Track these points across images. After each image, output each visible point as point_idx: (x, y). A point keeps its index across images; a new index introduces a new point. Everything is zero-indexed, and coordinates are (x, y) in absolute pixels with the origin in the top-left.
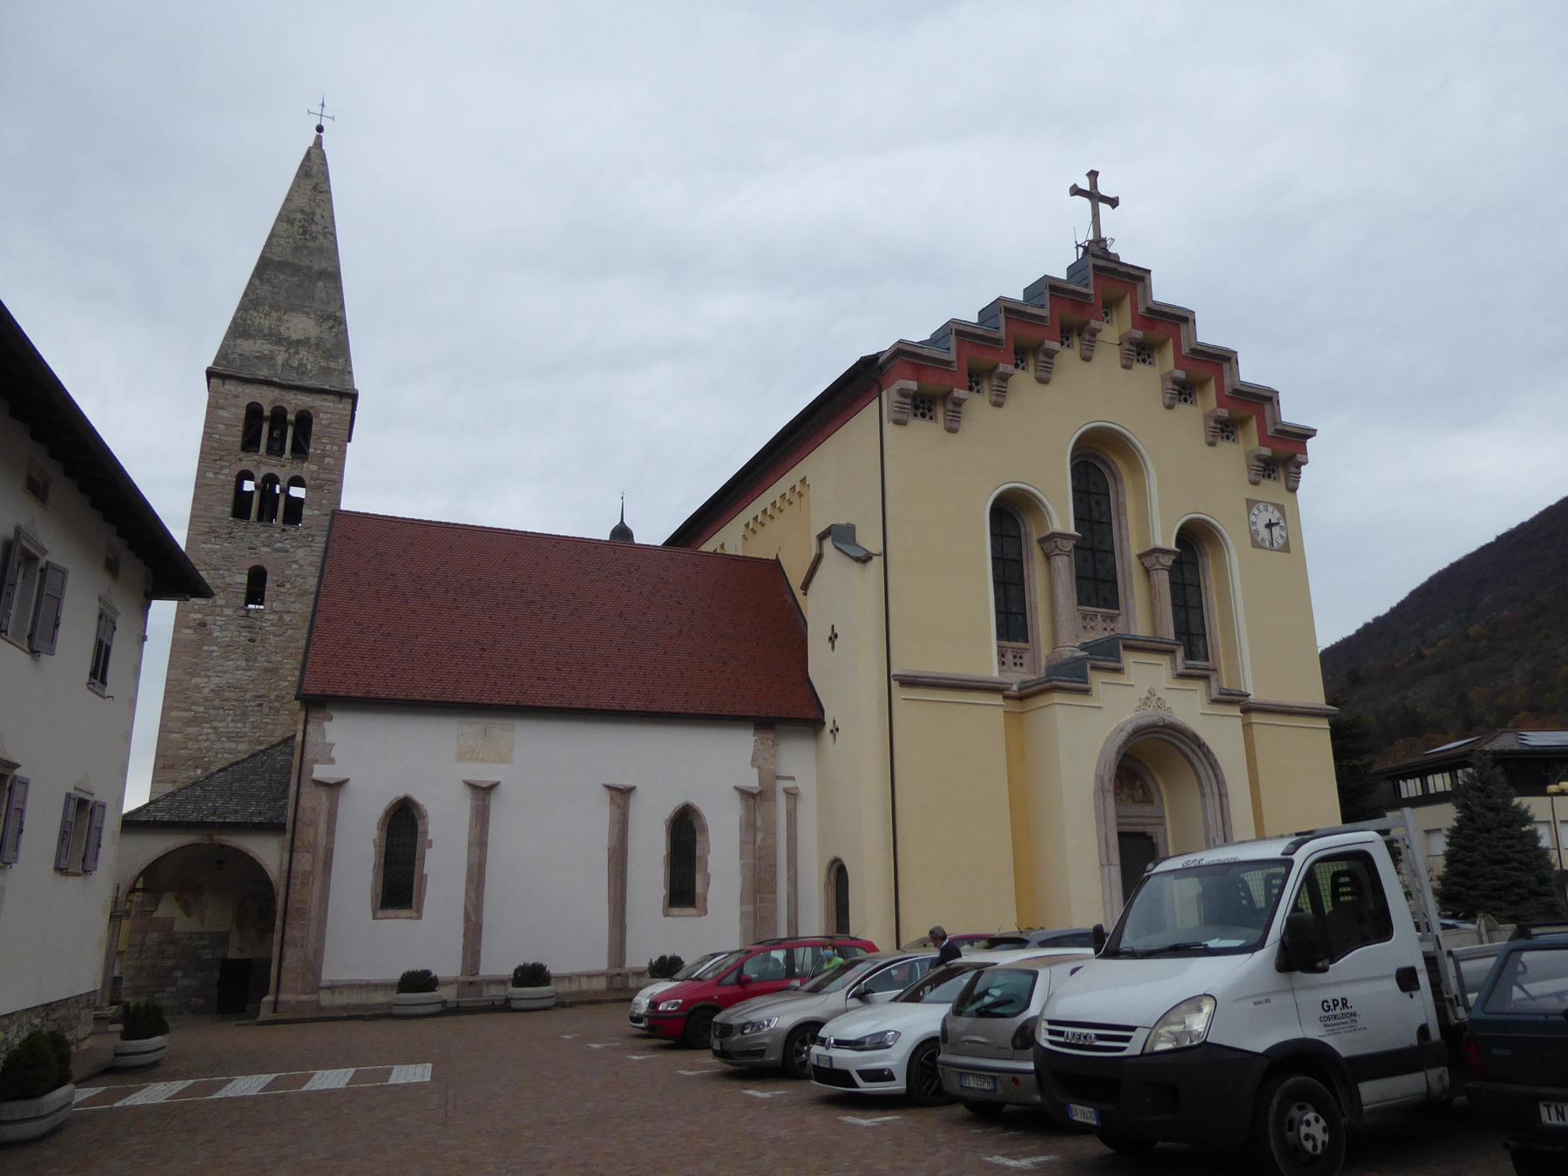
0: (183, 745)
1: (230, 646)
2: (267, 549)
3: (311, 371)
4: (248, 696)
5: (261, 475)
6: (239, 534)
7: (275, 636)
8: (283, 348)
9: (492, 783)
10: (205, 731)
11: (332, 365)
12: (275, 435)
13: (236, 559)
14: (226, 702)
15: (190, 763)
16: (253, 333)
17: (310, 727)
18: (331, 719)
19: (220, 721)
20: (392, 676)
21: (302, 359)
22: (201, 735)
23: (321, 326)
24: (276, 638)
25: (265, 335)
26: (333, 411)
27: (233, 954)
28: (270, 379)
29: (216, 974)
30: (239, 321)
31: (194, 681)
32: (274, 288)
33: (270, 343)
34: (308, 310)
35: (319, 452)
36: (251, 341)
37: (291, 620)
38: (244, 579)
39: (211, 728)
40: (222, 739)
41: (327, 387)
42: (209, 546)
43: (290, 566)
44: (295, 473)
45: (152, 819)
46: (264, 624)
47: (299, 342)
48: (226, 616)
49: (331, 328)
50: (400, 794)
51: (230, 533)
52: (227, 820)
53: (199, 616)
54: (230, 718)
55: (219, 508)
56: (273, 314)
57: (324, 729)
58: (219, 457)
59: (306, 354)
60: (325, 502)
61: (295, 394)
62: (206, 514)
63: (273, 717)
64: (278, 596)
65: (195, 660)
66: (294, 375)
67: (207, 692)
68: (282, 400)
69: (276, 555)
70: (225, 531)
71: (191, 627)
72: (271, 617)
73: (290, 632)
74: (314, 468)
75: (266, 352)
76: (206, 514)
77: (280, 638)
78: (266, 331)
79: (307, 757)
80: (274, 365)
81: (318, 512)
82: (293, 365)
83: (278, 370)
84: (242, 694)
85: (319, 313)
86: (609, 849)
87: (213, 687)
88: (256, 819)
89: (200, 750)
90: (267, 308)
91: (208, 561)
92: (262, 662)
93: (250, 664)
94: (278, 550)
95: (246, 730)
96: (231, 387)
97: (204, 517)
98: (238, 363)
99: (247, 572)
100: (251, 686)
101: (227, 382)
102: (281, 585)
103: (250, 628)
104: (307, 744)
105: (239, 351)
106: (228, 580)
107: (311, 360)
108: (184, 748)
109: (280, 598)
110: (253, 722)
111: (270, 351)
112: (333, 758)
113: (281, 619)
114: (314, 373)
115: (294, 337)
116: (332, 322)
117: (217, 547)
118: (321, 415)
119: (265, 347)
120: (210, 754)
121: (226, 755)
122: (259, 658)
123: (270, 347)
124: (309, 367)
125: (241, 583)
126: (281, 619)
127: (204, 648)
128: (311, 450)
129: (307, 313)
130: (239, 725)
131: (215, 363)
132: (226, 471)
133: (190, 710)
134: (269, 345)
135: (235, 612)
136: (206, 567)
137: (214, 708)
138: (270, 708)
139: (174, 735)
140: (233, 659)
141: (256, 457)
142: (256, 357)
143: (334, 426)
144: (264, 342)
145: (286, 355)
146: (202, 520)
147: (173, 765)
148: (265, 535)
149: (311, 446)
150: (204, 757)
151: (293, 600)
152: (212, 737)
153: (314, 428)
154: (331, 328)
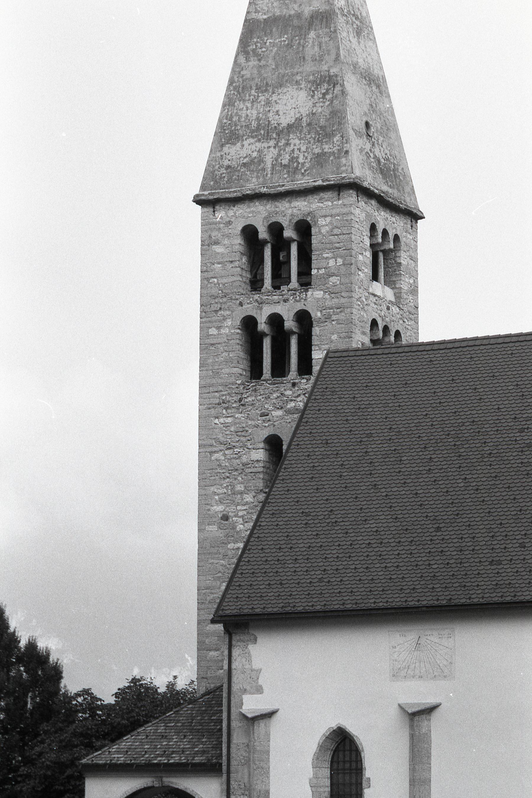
2: (280, 413)
3: (303, 164)
6: (250, 399)
8: (272, 143)
9: (427, 706)
11: (327, 148)
12: (281, 258)
16: (241, 132)
17: (236, 652)
18: (255, 641)
20: (320, 580)
21: (293, 150)
23: (313, 96)
25: (253, 131)
26: (334, 212)
28: (257, 191)
30: (225, 121)
32: (259, 60)
33: (259, 140)
34: (298, 78)
35: (322, 271)
36: (239, 144)
41: (320, 183)
42: (222, 420)
44: (299, 306)
45: (108, 762)
47: (290, 127)
48: (247, 503)
49: (324, 95)
50: (334, 725)
51: (240, 400)
52: (170, 762)
56: (262, 98)
57: (249, 653)
59: (297, 142)
66: (286, 176)
70: (235, 398)
74: (319, 294)
75: (255, 154)
76: (214, 381)
78: (254, 124)
79: (235, 687)
80: (264, 169)
82: (284, 162)
83: (267, 174)
85: (311, 78)
88: (198, 759)
90: (253, 92)
91: (222, 439)
96: (221, 214)
97: (212, 385)
98: (226, 179)
99: (262, 445)
101: (217, 207)
104: (234, 672)
105: (226, 163)
106: (244, 459)
107: (303, 149)
111: (259, 151)
112: (261, 687)
114: (307, 165)
115: (285, 121)
116: (326, 86)
117: (230, 420)
118: (321, 222)
119: (253, 147)
123: (259, 145)
124: (301, 160)
125: (258, 461)
127: (229, 546)
128: (314, 272)
129: (297, 83)
131: (203, 187)
132: (229, 322)
134: (257, 144)
135: (254, 497)
136: (222, 447)
141: (256, 297)
142: (244, 165)
143: (336, 231)
144: (252, 140)
145: (276, 152)
149: (313, 266)
153: (315, 241)
154: (324, 95)
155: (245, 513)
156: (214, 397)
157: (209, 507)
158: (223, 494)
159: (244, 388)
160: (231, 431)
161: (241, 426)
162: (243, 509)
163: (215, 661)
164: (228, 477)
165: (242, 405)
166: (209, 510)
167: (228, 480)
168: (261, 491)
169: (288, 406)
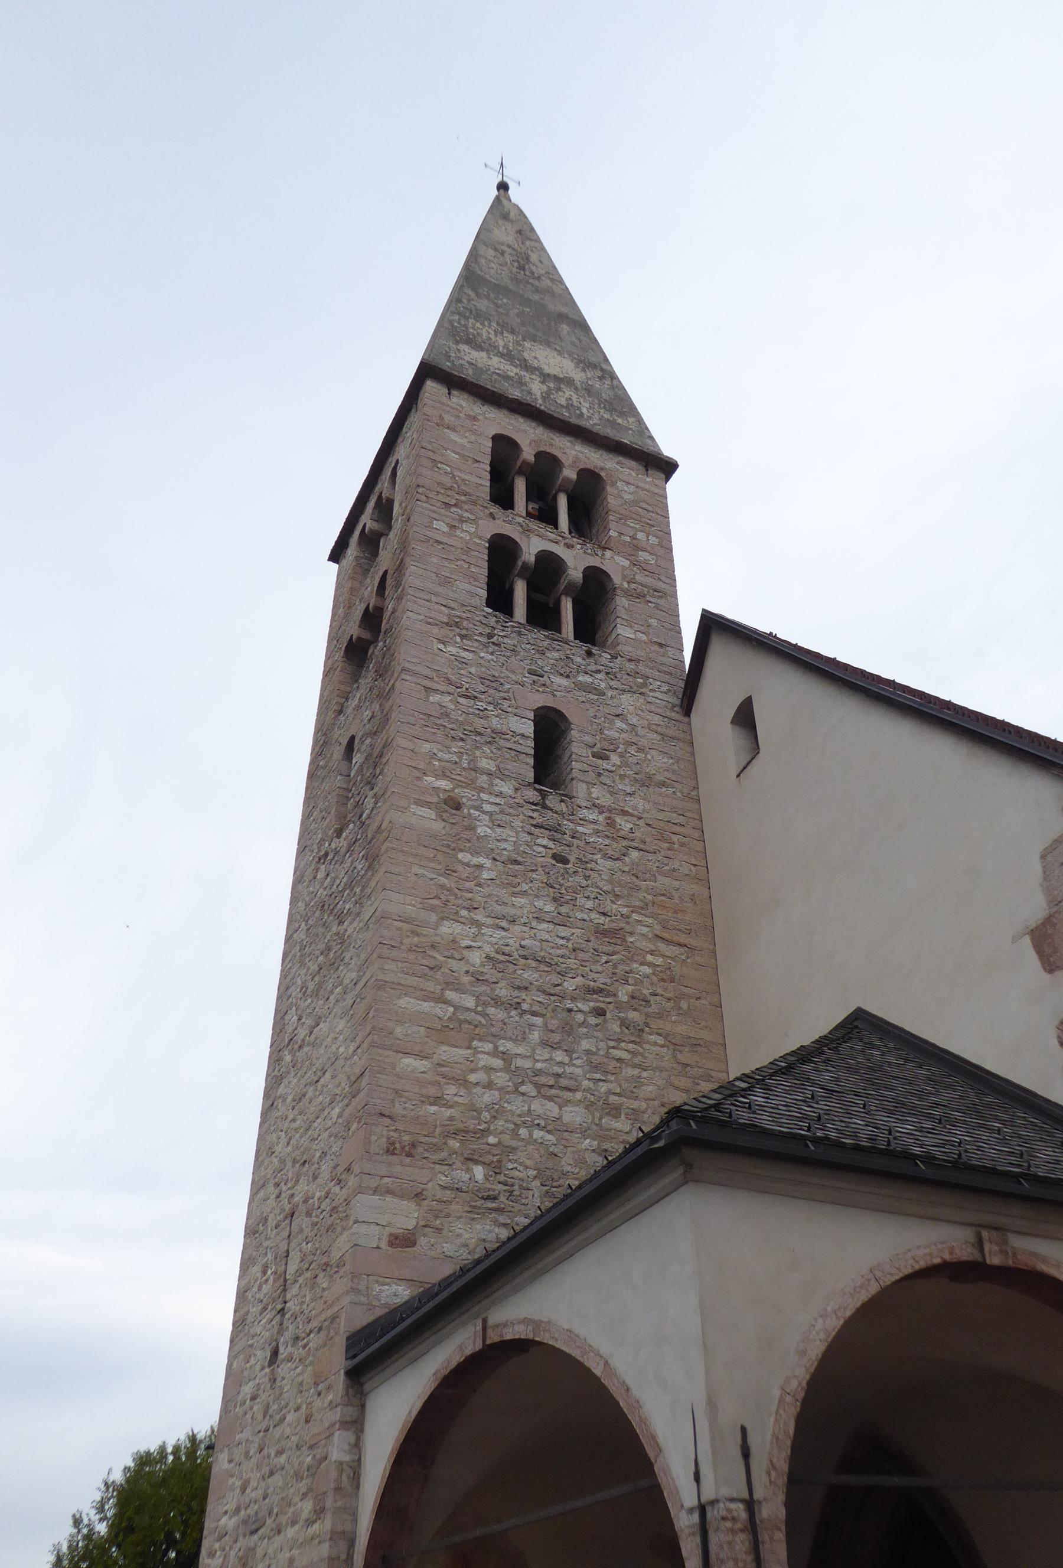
0: (432, 1091)
2: (564, 682)
4: (570, 985)
5: (534, 551)
7: (606, 856)
10: (485, 1060)
13: (507, 686)
14: (523, 995)
15: (454, 1144)
19: (515, 1041)
22: (473, 1071)
24: (609, 864)
31: (447, 929)
37: (631, 830)
38: (529, 728)
39: (495, 1053)
40: (523, 1089)
43: (612, 722)
46: (580, 829)
48: (500, 795)
53: (443, 784)
55: (463, 585)
58: (453, 502)
60: (653, 622)
61: (571, 442)
62: (440, 589)
63: (631, 1046)
64: (599, 775)
65: (443, 880)
67: (477, 961)
68: (552, 445)
69: (582, 696)
71: (428, 804)
72: (592, 816)
73: (634, 854)
76: (440, 589)
77: (618, 864)
81: (644, 638)
84: (555, 978)
87: (488, 949)
89: (473, 1108)
92: (585, 910)
97: (436, 594)
99: (531, 715)
100: (572, 963)
102: (602, 756)
103: (554, 830)
108: (437, 1100)
109: (603, 779)
110: (588, 1052)
113: (611, 823)
117: (469, 656)
120: (500, 1123)
121: (538, 1134)
122: (581, 900)
125: (523, 735)
126: (611, 823)
127: (460, 856)
130: (559, 1056)
133: (442, 1000)
135: (516, 789)
136: (451, 689)
137: (497, 1002)
138: (624, 1024)
140: (524, 893)
146: (434, 598)
147: (413, 1145)
148: (556, 655)
150: (486, 1132)
151: (628, 790)
152: (502, 1079)
155: (497, 809)
156: (440, 612)
159: (497, 622)
160: (470, 673)
161: (490, 673)
162: (491, 800)
163: (418, 1080)
164: (462, 740)
165: (493, 643)
167: (461, 743)
169: (580, 678)
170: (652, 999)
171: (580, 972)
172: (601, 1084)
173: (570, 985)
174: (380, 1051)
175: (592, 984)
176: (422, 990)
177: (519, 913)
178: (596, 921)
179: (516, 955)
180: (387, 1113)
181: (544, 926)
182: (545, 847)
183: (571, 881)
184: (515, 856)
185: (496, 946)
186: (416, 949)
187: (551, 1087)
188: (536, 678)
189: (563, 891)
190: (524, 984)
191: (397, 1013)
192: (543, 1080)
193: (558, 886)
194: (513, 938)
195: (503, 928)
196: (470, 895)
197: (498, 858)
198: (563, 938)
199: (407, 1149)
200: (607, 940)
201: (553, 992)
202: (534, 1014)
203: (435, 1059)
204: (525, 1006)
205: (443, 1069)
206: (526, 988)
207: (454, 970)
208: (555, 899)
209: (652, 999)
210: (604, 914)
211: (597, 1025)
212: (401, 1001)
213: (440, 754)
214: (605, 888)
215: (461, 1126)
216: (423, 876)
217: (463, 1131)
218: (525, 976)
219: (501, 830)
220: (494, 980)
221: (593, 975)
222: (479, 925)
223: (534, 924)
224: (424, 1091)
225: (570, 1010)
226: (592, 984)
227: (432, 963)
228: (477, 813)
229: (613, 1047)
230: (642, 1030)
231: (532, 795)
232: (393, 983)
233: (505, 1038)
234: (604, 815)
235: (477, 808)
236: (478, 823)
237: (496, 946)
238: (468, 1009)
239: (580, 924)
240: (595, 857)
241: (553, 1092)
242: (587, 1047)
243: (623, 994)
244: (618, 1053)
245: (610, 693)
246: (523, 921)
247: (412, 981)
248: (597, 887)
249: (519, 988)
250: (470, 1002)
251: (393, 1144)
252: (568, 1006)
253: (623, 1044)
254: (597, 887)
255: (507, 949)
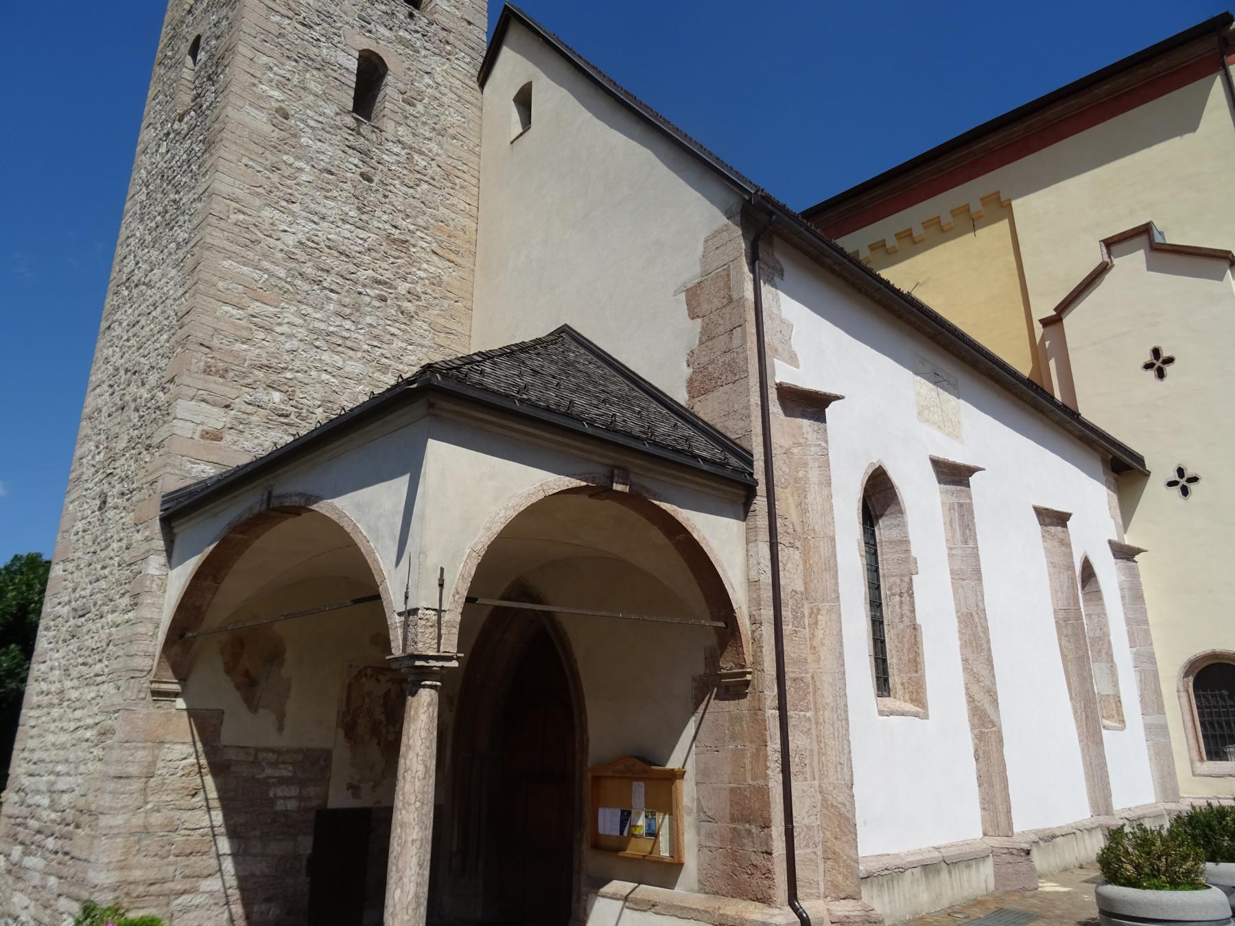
0: (245, 334)
1: (331, 173)
2: (387, 33)
4: (363, 275)
13: (339, 24)
14: (325, 275)
15: (260, 374)
24: (405, 189)
27: (339, 799)
29: (306, 845)
31: (267, 213)
38: (353, 65)
43: (422, 77)
46: (385, 157)
54: (332, 307)
64: (406, 118)
67: (291, 243)
73: (425, 186)
77: (411, 191)
84: (352, 268)
86: (1055, 611)
87: (301, 236)
93: (364, 217)
94: (401, 41)
95: (361, 337)
99: (357, 54)
109: (409, 122)
110: (370, 325)
113: (409, 158)
121: (325, 376)
122: (378, 213)
125: (347, 69)
126: (409, 158)
130: (348, 324)
136: (290, 14)
139: (226, 308)
140: (334, 199)
151: (427, 134)
152: (301, 333)
155: (319, 126)
157: (256, 81)
158: (285, 77)
162: (315, 118)
163: (234, 324)
166: (254, 85)
167: (294, 64)
168: (349, 112)
169: (401, 33)
170: (423, 296)
171: (371, 266)
172: (377, 349)
173: (363, 275)
174: (205, 298)
175: (380, 277)
176: (243, 257)
177: (329, 213)
178: (389, 231)
179: (322, 245)
180: (206, 343)
181: (348, 226)
182: (356, 166)
183: (372, 198)
184: (330, 167)
185: (308, 235)
186: (241, 224)
187: (339, 345)
188: (364, 24)
189: (366, 203)
190: (326, 267)
191: (220, 271)
192: (334, 339)
193: (362, 199)
194: (325, 231)
195: (315, 222)
196: (290, 191)
197: (316, 165)
198: (361, 239)
199: (221, 372)
200: (395, 247)
201: (348, 277)
202: (332, 291)
203: (250, 311)
204: (325, 284)
205: (255, 319)
206: (328, 271)
207: (271, 246)
208: (359, 209)
209: (423, 296)
210: (396, 227)
211: (379, 307)
212: (225, 262)
213: (275, 69)
214: (399, 208)
215: (266, 362)
216: (252, 167)
217: (267, 366)
218: (328, 261)
219: (320, 144)
220: (303, 260)
221: (380, 271)
222: (293, 214)
223: (340, 223)
224: (238, 333)
225: (360, 293)
226: (380, 277)
227: (254, 238)
228: (302, 126)
229: (389, 325)
230: (412, 317)
231: (349, 120)
232: (219, 247)
233: (307, 305)
234: (406, 151)
235: (303, 121)
236: (303, 134)
237: (308, 235)
238: (280, 278)
239: (376, 231)
240: (394, 182)
241: (340, 349)
242: (370, 322)
243: (403, 287)
244: (393, 330)
245: (423, 52)
246: (331, 219)
247: (235, 248)
248: (393, 205)
249: (323, 270)
250: (282, 273)
251: (209, 367)
252: (359, 290)
253: (397, 324)
254: (393, 205)
255: (316, 239)
